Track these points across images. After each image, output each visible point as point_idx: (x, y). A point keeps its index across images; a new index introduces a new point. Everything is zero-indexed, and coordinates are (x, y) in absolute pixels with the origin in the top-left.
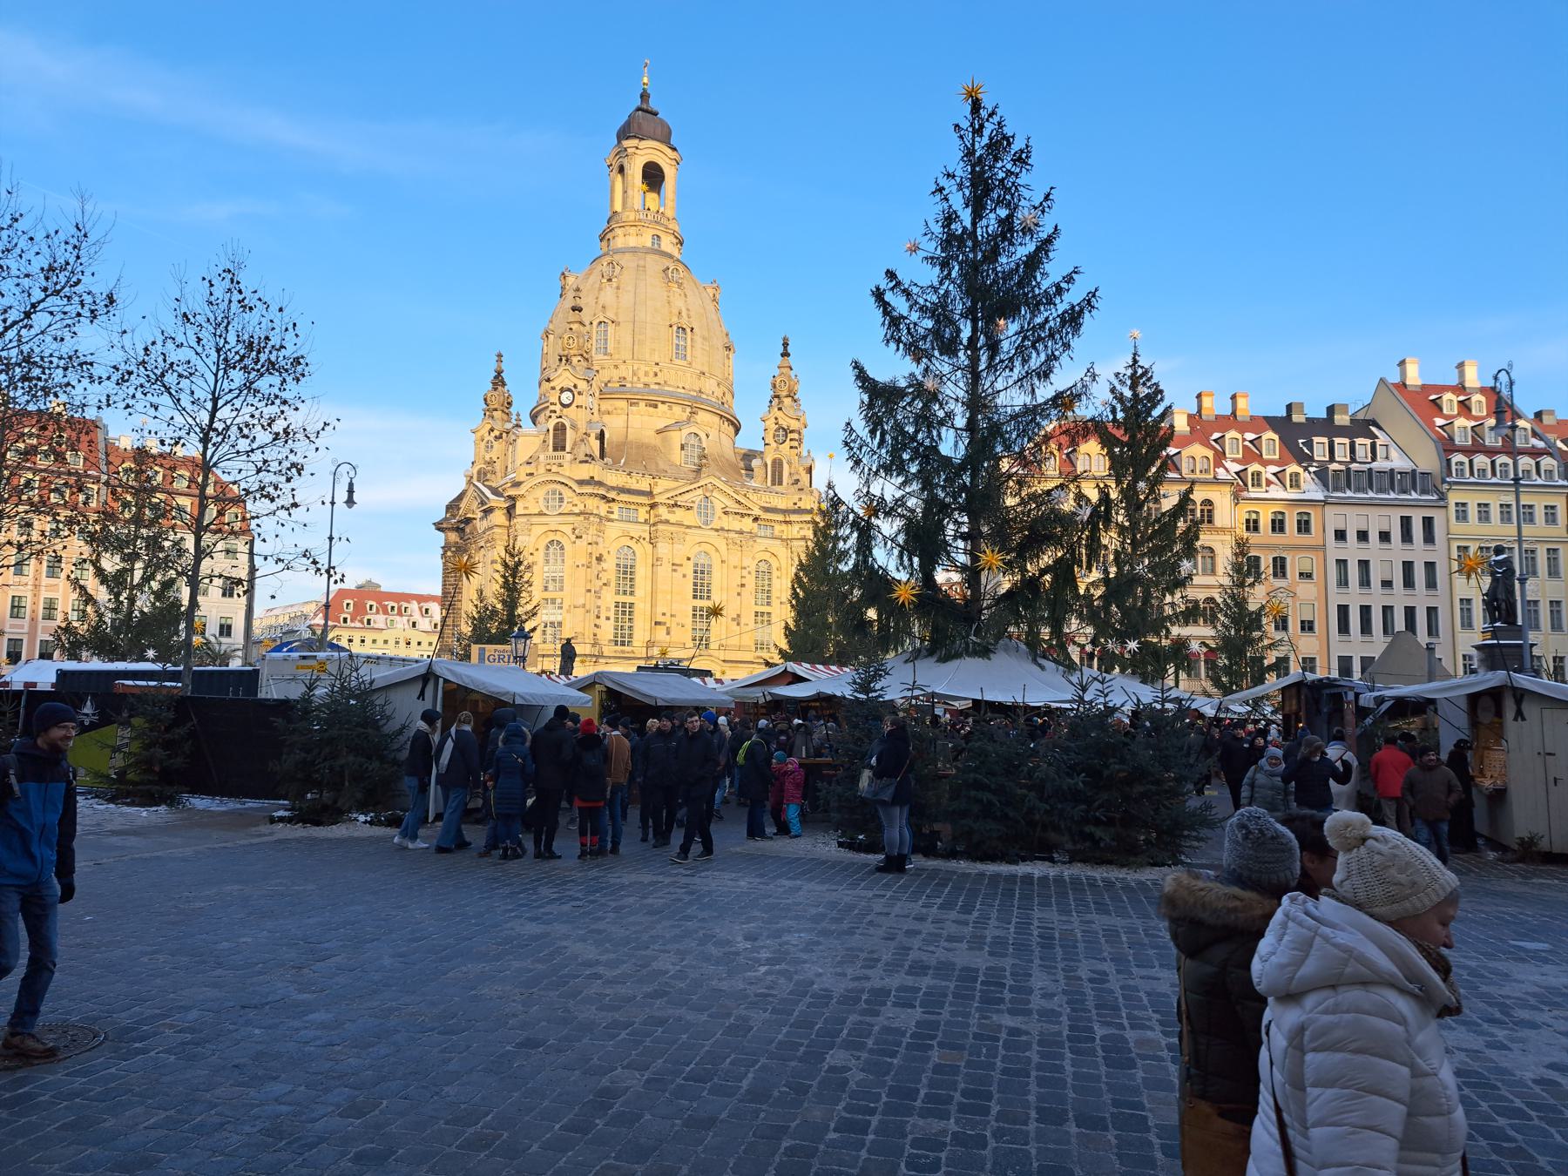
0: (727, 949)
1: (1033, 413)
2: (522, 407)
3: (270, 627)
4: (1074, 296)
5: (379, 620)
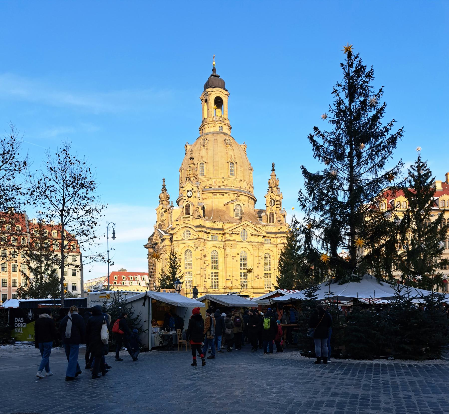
0: (260, 388)
1: (376, 182)
2: (173, 199)
3: (90, 287)
4: (393, 131)
5: (127, 283)
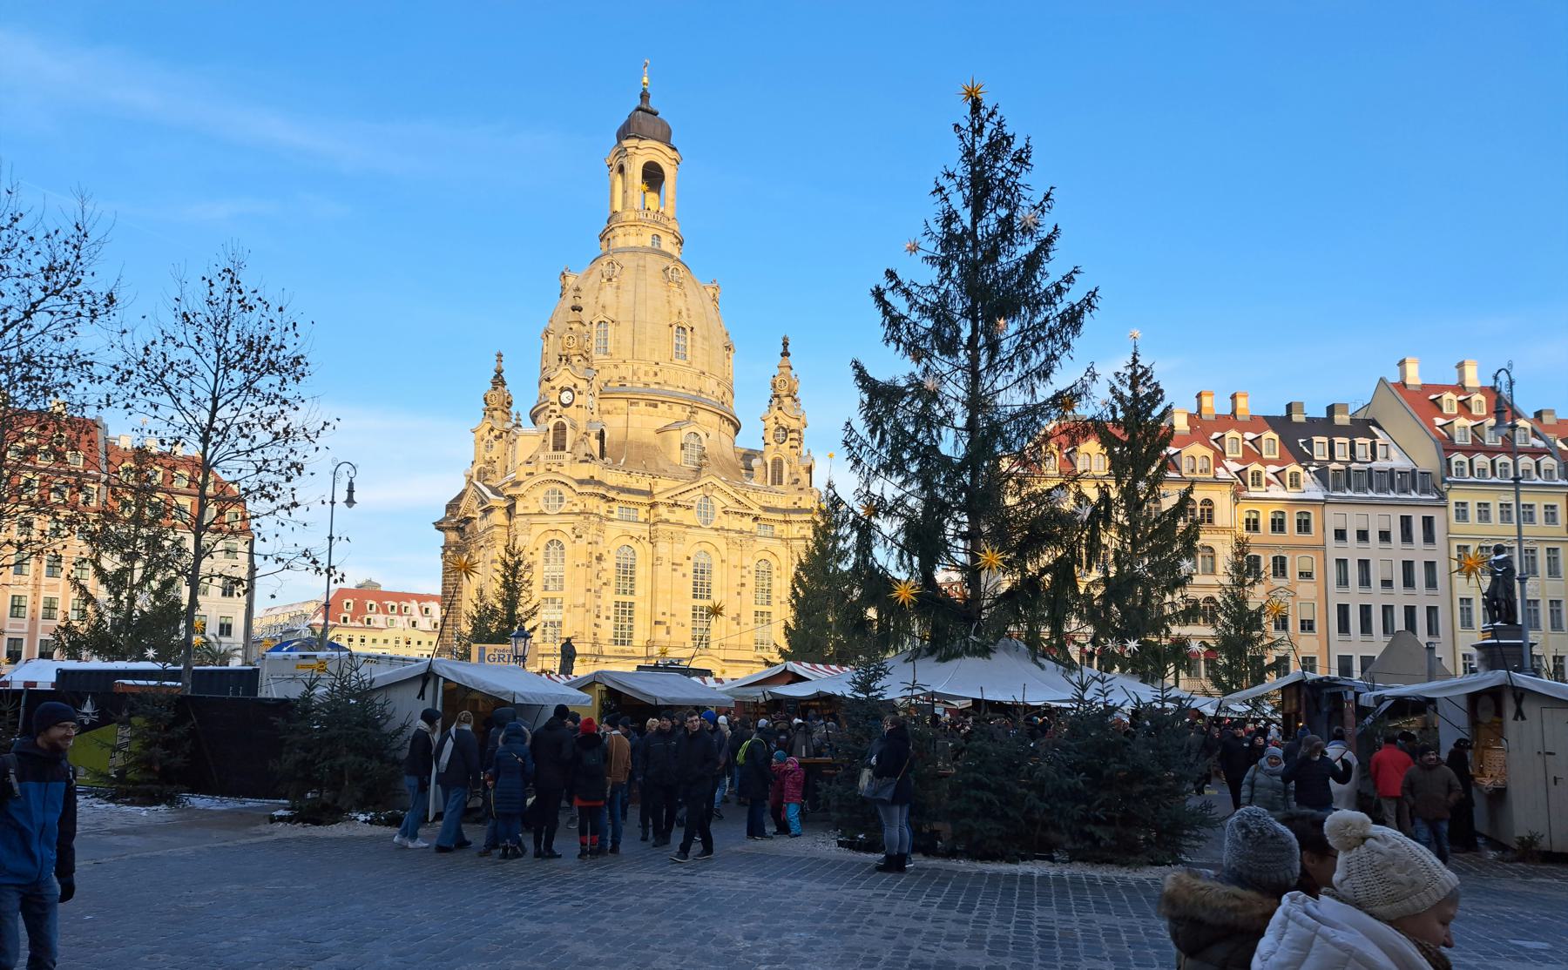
1: (1032, 412)
2: (522, 407)
3: (270, 627)
4: (1074, 296)
5: (379, 620)
